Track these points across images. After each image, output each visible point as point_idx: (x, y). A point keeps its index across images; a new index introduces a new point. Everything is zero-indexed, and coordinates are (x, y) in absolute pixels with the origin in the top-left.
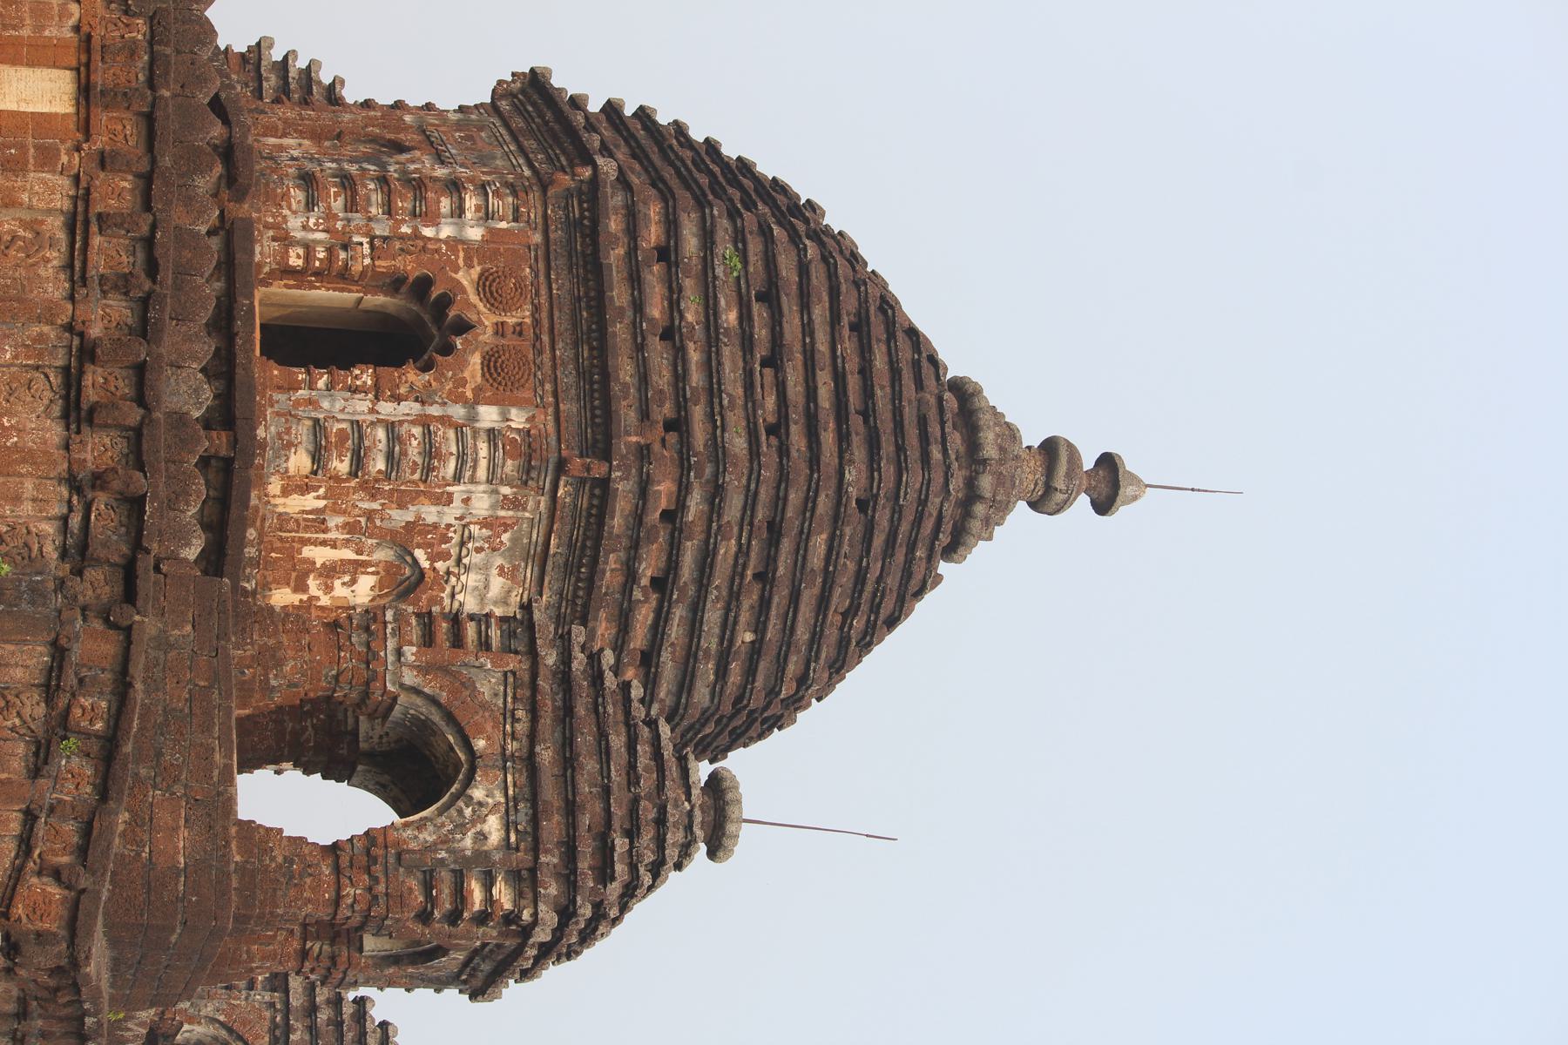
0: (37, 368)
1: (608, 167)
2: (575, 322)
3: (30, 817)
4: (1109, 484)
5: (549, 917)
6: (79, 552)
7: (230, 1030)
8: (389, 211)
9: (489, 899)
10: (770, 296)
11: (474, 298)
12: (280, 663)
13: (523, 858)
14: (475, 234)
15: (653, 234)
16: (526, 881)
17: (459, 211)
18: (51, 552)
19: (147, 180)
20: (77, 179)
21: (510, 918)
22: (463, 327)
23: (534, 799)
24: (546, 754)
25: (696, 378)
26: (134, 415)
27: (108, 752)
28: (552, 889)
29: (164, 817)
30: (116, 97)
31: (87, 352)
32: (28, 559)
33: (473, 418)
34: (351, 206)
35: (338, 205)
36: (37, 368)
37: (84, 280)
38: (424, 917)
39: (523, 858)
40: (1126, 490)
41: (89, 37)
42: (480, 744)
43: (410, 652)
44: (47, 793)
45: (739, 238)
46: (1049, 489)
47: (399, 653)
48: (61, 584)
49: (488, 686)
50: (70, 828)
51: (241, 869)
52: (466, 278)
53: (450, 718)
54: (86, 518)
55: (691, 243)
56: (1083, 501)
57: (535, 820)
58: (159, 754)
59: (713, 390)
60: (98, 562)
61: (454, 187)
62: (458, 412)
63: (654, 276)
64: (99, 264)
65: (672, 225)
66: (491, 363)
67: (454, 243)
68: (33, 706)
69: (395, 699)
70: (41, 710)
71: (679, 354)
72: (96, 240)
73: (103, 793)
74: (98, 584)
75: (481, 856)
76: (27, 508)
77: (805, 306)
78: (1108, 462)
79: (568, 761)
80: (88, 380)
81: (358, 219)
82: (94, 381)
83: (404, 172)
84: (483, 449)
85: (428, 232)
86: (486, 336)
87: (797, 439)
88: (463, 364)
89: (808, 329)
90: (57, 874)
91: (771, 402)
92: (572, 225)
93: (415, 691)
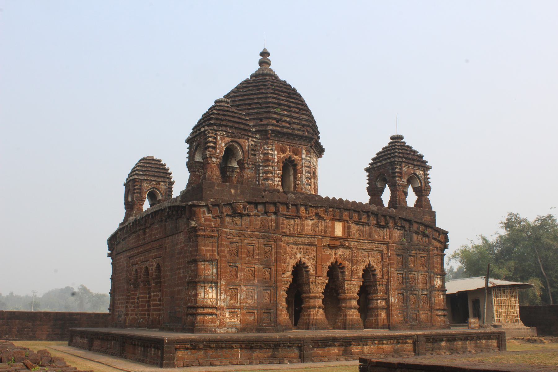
1: (270, 128)
2: (291, 139)
4: (265, 54)
6: (403, 227)
8: (273, 166)
10: (280, 105)
11: (285, 155)
14: (276, 152)
15: (274, 122)
17: (272, 155)
18: (401, 232)
19: (355, 211)
22: (290, 158)
24: (415, 163)
25: (296, 121)
30: (341, 216)
32: (403, 236)
33: (304, 159)
34: (272, 173)
35: (271, 175)
39: (425, 169)
44: (431, 236)
45: (273, 108)
48: (405, 230)
50: (434, 233)
52: (282, 156)
55: (275, 116)
59: (299, 119)
61: (266, 154)
62: (304, 161)
64: (366, 221)
65: (274, 119)
66: (295, 154)
67: (277, 157)
71: (294, 123)
72: (362, 220)
74: (407, 225)
77: (279, 99)
78: (262, 54)
79: (413, 160)
80: (381, 224)
83: (262, 162)
84: (308, 158)
85: (276, 160)
86: (291, 154)
87: (300, 106)
88: (295, 159)
89: (283, 100)
90: (439, 235)
91: (296, 110)
92: (276, 136)
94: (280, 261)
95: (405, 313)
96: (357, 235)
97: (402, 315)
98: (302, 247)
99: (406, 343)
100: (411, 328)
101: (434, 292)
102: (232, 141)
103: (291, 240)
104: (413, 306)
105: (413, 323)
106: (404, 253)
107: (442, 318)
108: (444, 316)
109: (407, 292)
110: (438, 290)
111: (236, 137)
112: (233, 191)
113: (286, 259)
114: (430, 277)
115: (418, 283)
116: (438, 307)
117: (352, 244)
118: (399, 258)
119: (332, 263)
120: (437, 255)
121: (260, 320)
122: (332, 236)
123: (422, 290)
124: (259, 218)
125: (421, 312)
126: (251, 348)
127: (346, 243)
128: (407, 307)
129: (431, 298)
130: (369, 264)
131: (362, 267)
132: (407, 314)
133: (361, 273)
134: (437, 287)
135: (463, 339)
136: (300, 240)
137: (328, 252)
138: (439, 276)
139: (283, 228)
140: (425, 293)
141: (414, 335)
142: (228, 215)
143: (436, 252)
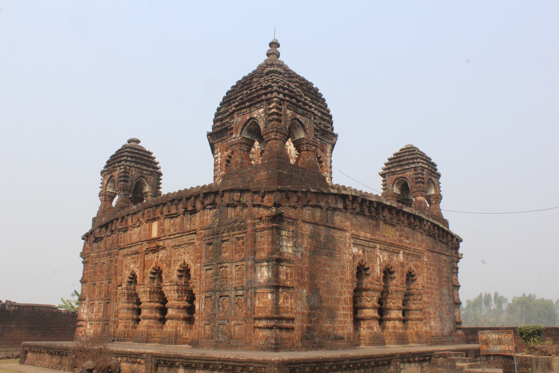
0: (191, 220)
3: (254, 206)
4: (274, 45)
5: (275, 94)
6: (214, 205)
7: (394, 183)
9: (273, 108)
12: (237, 161)
13: (265, 103)
14: (220, 154)
16: (269, 101)
18: (215, 211)
20: (165, 218)
21: (277, 102)
23: (255, 104)
24: (247, 104)
26: (193, 198)
27: (242, 191)
28: (269, 95)
29: (258, 178)
30: (155, 214)
31: (186, 210)
32: (215, 215)
36: (191, 220)
37: (177, 213)
38: (280, 121)
39: (265, 103)
40: (274, 41)
41: (147, 220)
42: (248, 118)
43: (234, 136)
46: (273, 53)
47: (234, 138)
48: (219, 208)
49: (239, 119)
50: (256, 197)
51: (268, 160)
53: (245, 125)
54: (208, 205)
56: (278, 49)
57: (258, 102)
58: (249, 182)
60: (214, 201)
63: (224, 121)
68: (238, 208)
69: (244, 137)
70: (238, 207)
72: (172, 212)
73: (248, 190)
75: (265, 112)
76: (209, 217)
78: (271, 44)
81: (218, 175)
82: (190, 208)
90: (263, 197)
92: (218, 138)
93: (241, 133)
94: (116, 274)
95: (212, 324)
96: (172, 230)
97: (209, 326)
98: (133, 256)
99: (139, 363)
100: (217, 346)
101: (250, 290)
102: (112, 176)
103: (125, 251)
104: (222, 315)
105: (221, 339)
106: (214, 238)
107: (267, 333)
108: (270, 328)
109: (215, 294)
110: (261, 287)
111: (112, 172)
112: (104, 219)
113: (122, 271)
114: (247, 267)
115: (231, 279)
116: (260, 315)
117: (166, 243)
118: (211, 247)
119: (154, 268)
120: (263, 229)
121: (103, 330)
122: (148, 239)
123: (236, 289)
124: (110, 238)
125: (233, 323)
126: (51, 354)
127: (161, 244)
128: (215, 315)
129: (246, 301)
130: (184, 263)
131: (177, 267)
132: (213, 326)
133: (175, 277)
134: (262, 281)
135: (202, 366)
136: (130, 250)
137: (150, 256)
138: (265, 264)
139: (121, 242)
140: (240, 292)
141: (144, 353)
142: (94, 242)
143: (262, 225)
